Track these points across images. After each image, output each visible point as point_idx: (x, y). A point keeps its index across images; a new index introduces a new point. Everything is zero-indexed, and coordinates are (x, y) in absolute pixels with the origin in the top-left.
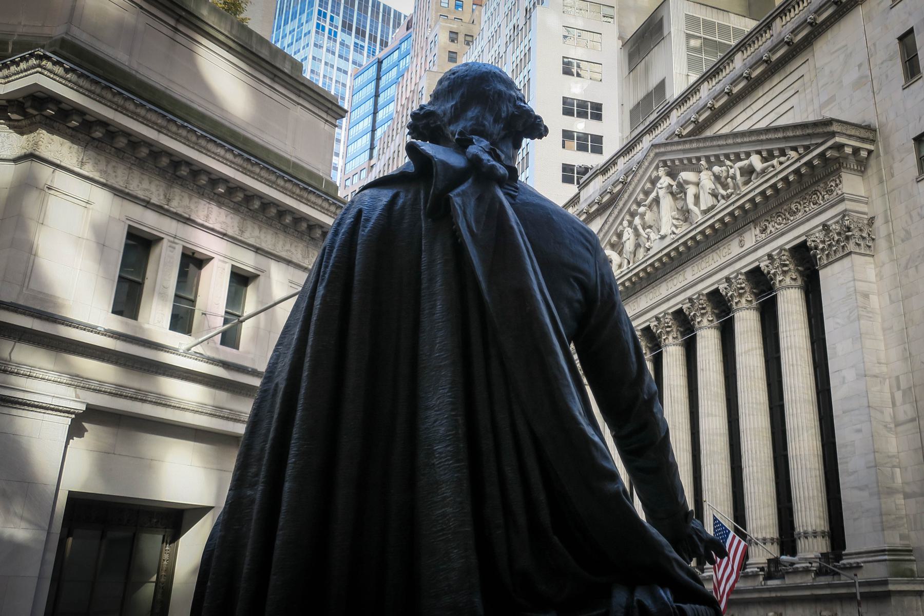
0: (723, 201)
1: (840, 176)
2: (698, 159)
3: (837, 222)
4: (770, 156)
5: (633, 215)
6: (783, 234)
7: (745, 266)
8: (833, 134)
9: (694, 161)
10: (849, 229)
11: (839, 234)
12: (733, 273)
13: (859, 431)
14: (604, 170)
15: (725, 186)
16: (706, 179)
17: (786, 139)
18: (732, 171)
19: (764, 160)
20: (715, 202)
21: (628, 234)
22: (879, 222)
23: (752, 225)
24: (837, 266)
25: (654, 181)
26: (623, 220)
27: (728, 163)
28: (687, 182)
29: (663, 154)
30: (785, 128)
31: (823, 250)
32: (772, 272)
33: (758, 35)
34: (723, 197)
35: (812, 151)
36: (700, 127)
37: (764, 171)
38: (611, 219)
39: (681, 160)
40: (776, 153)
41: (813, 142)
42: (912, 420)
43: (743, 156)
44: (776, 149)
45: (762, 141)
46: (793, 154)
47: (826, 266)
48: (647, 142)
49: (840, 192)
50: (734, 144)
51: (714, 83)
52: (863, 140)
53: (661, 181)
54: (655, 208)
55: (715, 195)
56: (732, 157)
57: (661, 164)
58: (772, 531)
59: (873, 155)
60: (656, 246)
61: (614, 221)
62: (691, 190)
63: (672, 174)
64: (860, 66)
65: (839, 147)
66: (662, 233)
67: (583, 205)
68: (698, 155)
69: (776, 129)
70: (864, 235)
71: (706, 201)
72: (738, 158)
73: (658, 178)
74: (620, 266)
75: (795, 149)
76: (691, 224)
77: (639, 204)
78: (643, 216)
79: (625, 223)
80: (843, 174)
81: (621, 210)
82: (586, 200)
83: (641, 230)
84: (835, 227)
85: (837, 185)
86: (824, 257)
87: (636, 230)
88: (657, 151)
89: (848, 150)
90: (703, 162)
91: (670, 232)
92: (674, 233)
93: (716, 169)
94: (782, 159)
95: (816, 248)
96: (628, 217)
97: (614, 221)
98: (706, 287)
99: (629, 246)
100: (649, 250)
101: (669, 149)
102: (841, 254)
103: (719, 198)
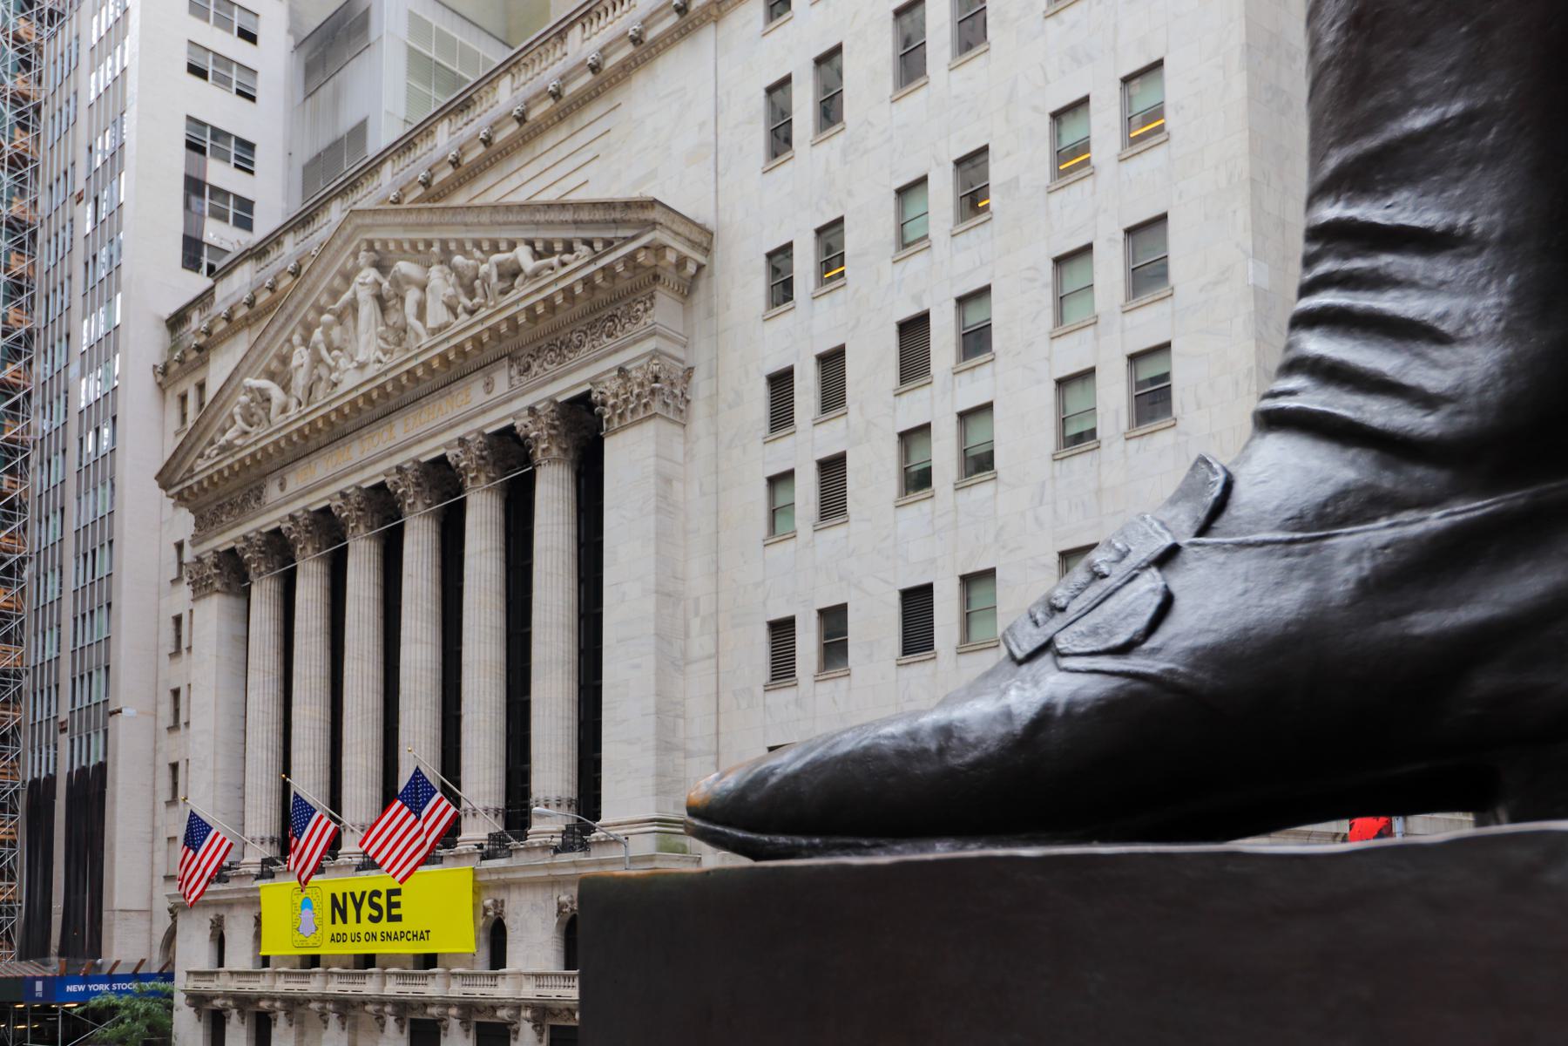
0: (464, 317)
1: (652, 297)
2: (429, 244)
3: (641, 367)
4: (549, 251)
5: (308, 329)
6: (554, 379)
7: (490, 424)
8: (654, 225)
9: (421, 247)
10: (656, 379)
11: (641, 385)
12: (470, 433)
13: (637, 666)
14: (258, 253)
15: (471, 293)
16: (440, 282)
17: (577, 224)
18: (484, 268)
19: (537, 255)
20: (452, 319)
21: (301, 357)
22: (699, 377)
23: (505, 361)
24: (631, 435)
25: (348, 277)
26: (293, 332)
27: (478, 254)
28: (409, 281)
29: (370, 227)
30: (578, 206)
31: (614, 407)
32: (533, 435)
33: (542, 49)
34: (465, 309)
35: (616, 249)
36: (432, 192)
37: (536, 274)
38: (272, 332)
39: (399, 244)
40: (558, 247)
41: (622, 233)
42: (709, 657)
43: (503, 246)
44: (558, 240)
45: (537, 223)
46: (583, 250)
47: (615, 432)
48: (336, 212)
49: (649, 321)
50: (493, 224)
51: (460, 124)
52: (694, 244)
53: (363, 274)
54: (349, 322)
55: (452, 309)
56: (486, 246)
57: (364, 246)
58: (496, 800)
59: (705, 272)
60: (350, 379)
61: (277, 333)
62: (412, 296)
63: (381, 266)
64: (702, 125)
65: (659, 249)
66: (361, 358)
67: (220, 307)
68: (428, 236)
69: (563, 206)
70: (677, 391)
71: (437, 314)
72: (495, 248)
73: (357, 270)
74: (284, 410)
75: (589, 243)
76: (408, 350)
77: (321, 311)
78: (328, 328)
79: (296, 339)
80: (658, 295)
81: (290, 317)
82: (225, 299)
83: (324, 353)
84: (637, 375)
85: (646, 310)
86: (616, 420)
87: (316, 351)
88: (359, 221)
89: (671, 257)
90: (436, 248)
91: (373, 358)
92: (380, 361)
93: (458, 259)
94: (566, 257)
95: (604, 404)
96: (300, 330)
97: (277, 333)
98: (428, 451)
99: (300, 380)
100: (335, 385)
101: (380, 219)
102: (642, 415)
103: (460, 309)
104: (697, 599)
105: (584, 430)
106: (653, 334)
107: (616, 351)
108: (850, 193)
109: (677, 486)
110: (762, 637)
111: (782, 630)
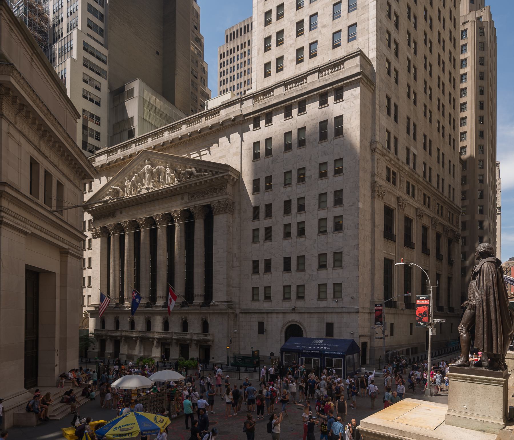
1: (226, 186)
11: (224, 205)
19: (197, 171)
40: (203, 171)
52: (236, 175)
104: (235, 254)
105: (209, 214)
106: (227, 194)
107: (217, 196)
108: (273, 171)
109: (231, 228)
110: (251, 263)
111: (256, 263)
